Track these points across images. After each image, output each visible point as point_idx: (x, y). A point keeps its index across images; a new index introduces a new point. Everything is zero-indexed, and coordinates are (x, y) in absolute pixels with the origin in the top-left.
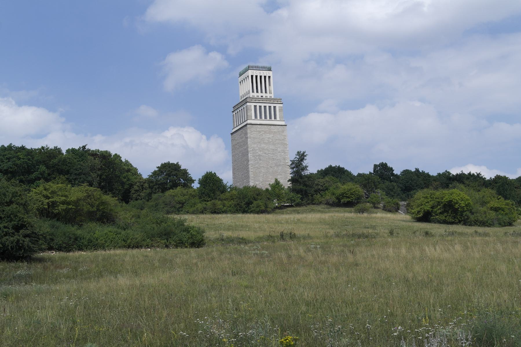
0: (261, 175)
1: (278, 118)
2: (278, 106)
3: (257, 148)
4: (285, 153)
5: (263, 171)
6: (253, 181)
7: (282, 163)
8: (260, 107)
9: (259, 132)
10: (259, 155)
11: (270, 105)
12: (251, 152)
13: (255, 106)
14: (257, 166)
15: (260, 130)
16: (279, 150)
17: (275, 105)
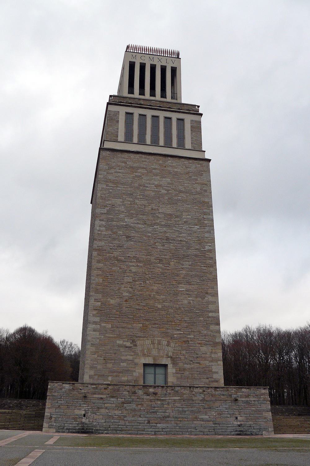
0: (127, 279)
1: (188, 145)
2: (188, 119)
3: (122, 209)
4: (203, 226)
5: (134, 269)
6: (99, 296)
7: (191, 252)
8: (143, 117)
9: (133, 169)
10: (127, 227)
11: (168, 114)
12: (103, 217)
13: (129, 115)
14: (116, 254)
15: (135, 165)
16: (185, 216)
17: (181, 116)
